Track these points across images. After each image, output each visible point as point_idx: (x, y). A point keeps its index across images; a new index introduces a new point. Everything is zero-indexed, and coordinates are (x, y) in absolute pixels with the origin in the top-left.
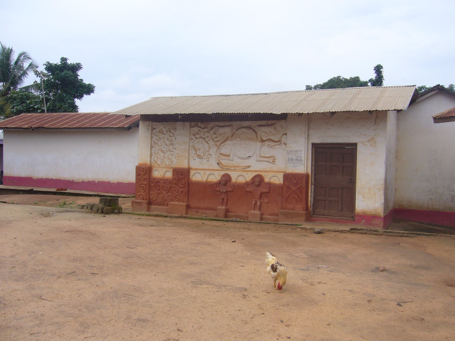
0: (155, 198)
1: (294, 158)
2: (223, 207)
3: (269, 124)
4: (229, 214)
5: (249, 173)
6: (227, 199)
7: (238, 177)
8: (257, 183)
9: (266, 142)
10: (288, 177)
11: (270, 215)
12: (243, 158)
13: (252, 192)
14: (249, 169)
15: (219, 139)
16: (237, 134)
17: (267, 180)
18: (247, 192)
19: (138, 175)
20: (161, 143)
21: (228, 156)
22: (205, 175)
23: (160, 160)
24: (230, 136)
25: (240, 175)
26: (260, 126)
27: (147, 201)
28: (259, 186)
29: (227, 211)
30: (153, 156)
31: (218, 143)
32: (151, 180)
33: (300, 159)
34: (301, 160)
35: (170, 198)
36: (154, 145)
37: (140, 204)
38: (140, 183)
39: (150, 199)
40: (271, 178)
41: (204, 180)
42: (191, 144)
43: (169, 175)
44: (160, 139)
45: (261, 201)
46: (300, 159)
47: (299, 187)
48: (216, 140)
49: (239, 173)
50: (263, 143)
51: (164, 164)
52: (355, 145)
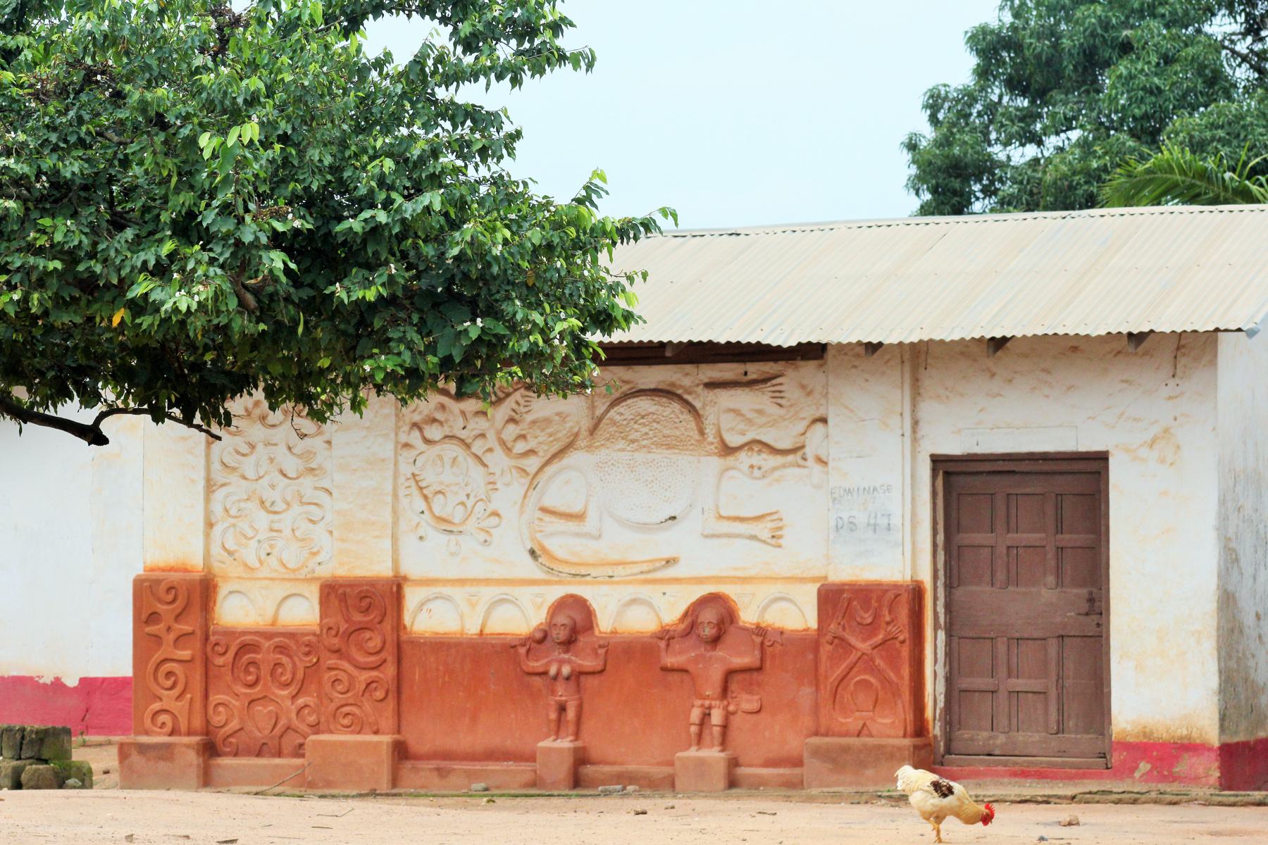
0: (234, 725)
1: (861, 519)
2: (565, 743)
3: (751, 376)
4: (589, 770)
5: (671, 589)
7: (625, 612)
8: (708, 632)
9: (742, 455)
10: (835, 600)
11: (769, 763)
12: (643, 527)
13: (686, 671)
14: (671, 572)
15: (532, 444)
16: (614, 423)
17: (748, 616)
18: (665, 669)
19: (145, 617)
20: (257, 465)
21: (579, 517)
22: (473, 606)
23: (253, 543)
24: (584, 433)
25: (634, 601)
26: (712, 385)
27: (195, 739)
28: (715, 641)
29: (581, 759)
30: (217, 530)
31: (532, 464)
32: (213, 639)
33: (883, 522)
34: (889, 528)
35: (312, 719)
36: (219, 475)
37: (165, 752)
38: (157, 657)
39: (208, 730)
41: (472, 629)
42: (406, 469)
43: (303, 612)
44: (252, 447)
45: (726, 708)
46: (883, 522)
47: (884, 642)
48: (520, 447)
49: (629, 592)
50: (730, 460)
51: (273, 561)
52: (1100, 460)
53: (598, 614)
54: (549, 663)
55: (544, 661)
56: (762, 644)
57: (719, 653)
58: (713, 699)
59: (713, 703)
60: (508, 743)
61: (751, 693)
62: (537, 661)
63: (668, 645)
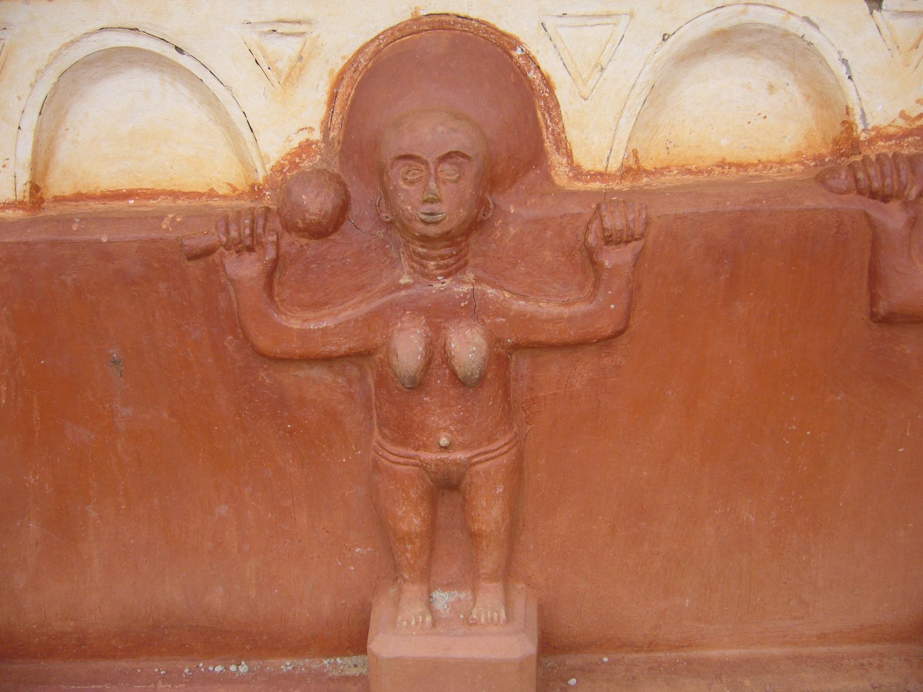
6: (517, 473)
53: (562, 95)
54: (382, 318)
55: (351, 311)
60: (216, 598)
62: (317, 305)
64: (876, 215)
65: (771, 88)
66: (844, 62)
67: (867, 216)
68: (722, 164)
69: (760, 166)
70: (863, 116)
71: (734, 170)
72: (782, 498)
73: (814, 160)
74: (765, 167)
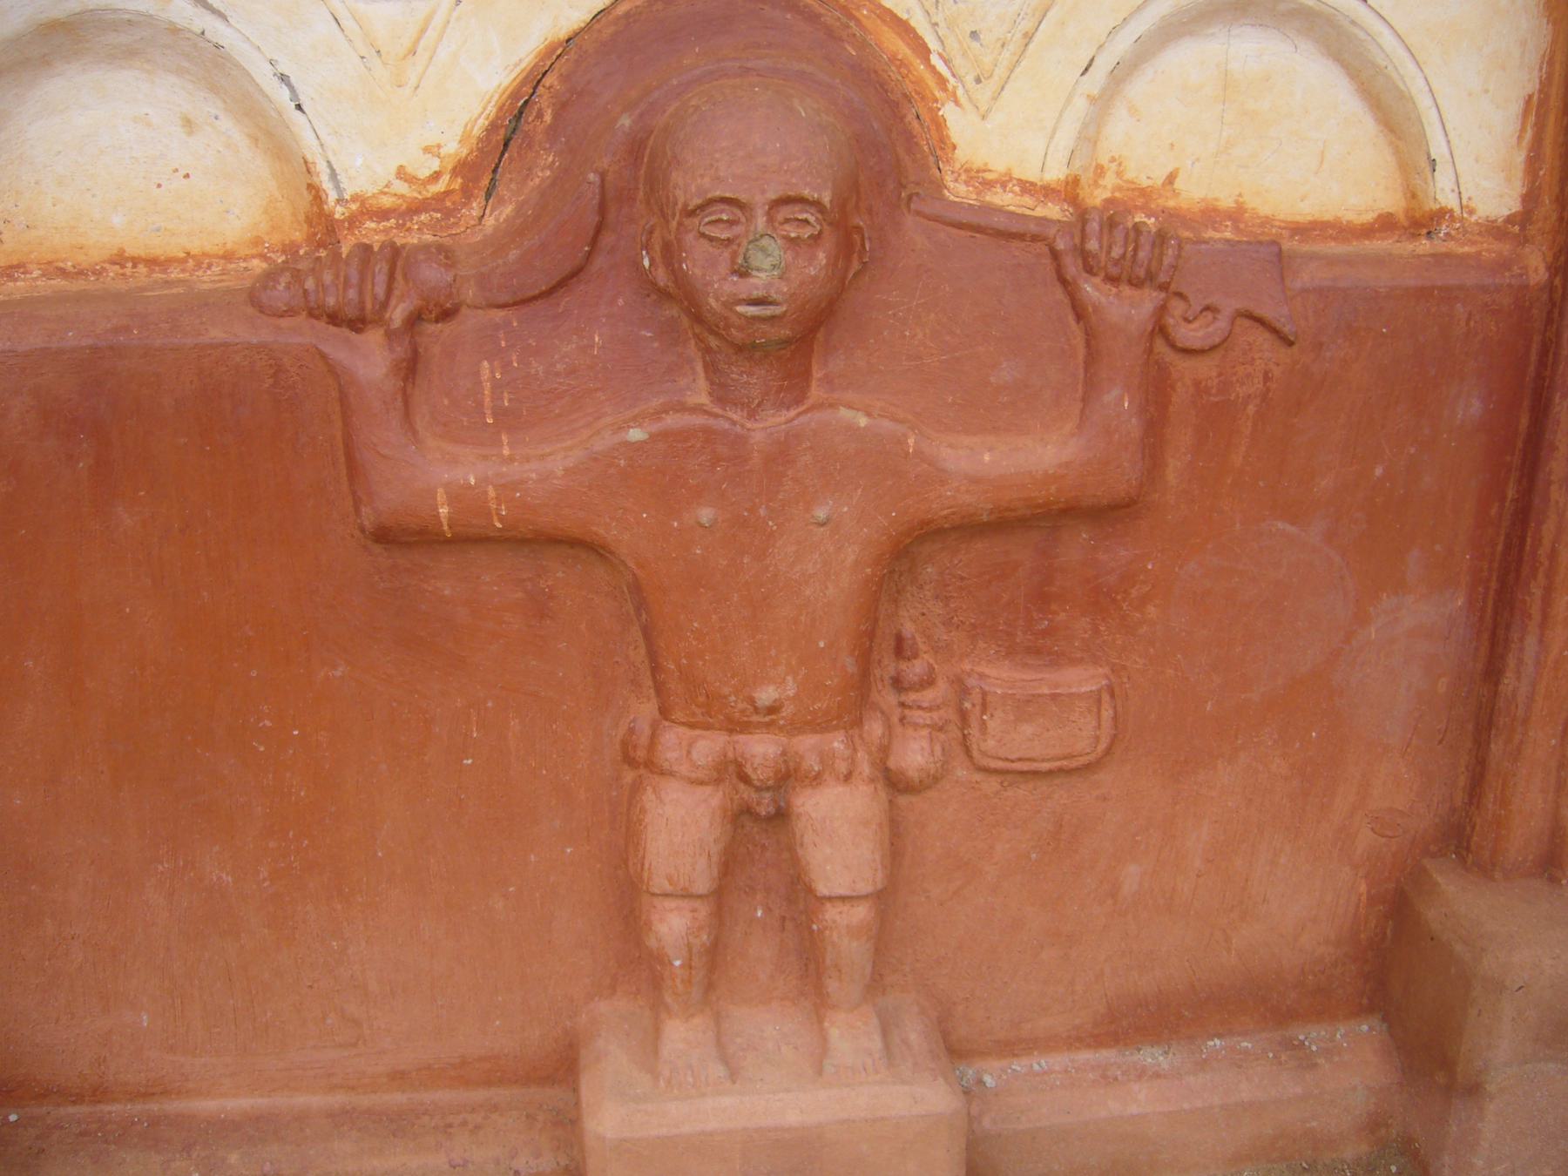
8: (774, 271)
11: (1136, 1022)
13: (586, 547)
18: (404, 538)
28: (796, 345)
40: (1122, 73)
56: (1160, 329)
57: (849, 412)
58: (799, 726)
59: (806, 743)
61: (1041, 648)
63: (410, 368)
64: (339, 354)
65: (188, 124)
66: (284, 78)
67: (324, 357)
68: (119, 259)
69: (191, 263)
70: (333, 175)
71: (142, 269)
72: (272, 844)
73: (284, 252)
74: (199, 265)
